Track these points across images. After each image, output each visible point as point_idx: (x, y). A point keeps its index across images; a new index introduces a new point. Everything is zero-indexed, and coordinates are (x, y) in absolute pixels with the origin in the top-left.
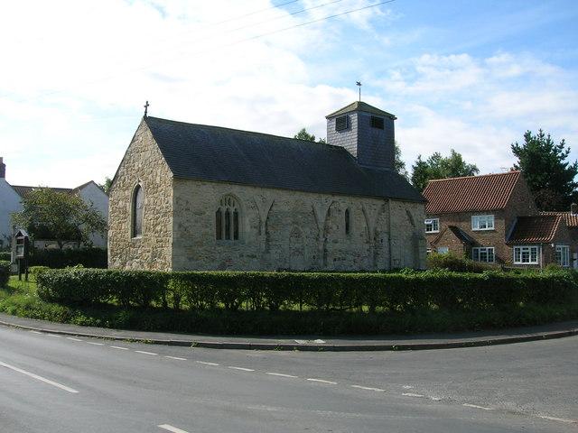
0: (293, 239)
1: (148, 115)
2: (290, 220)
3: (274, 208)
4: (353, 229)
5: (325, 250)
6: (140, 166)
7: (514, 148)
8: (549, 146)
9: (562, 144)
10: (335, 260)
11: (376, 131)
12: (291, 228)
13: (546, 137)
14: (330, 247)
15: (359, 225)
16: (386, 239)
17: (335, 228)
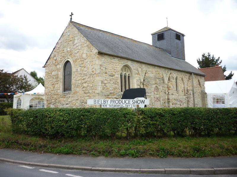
0: (156, 93)
1: (72, 20)
2: (154, 82)
3: (146, 75)
4: (179, 88)
5: (168, 99)
6: (69, 49)
7: (198, 62)
8: (213, 60)
9: (218, 59)
10: (173, 104)
11: (177, 41)
12: (154, 86)
13: (211, 56)
14: (171, 97)
15: (181, 86)
16: (192, 94)
17: (172, 87)
